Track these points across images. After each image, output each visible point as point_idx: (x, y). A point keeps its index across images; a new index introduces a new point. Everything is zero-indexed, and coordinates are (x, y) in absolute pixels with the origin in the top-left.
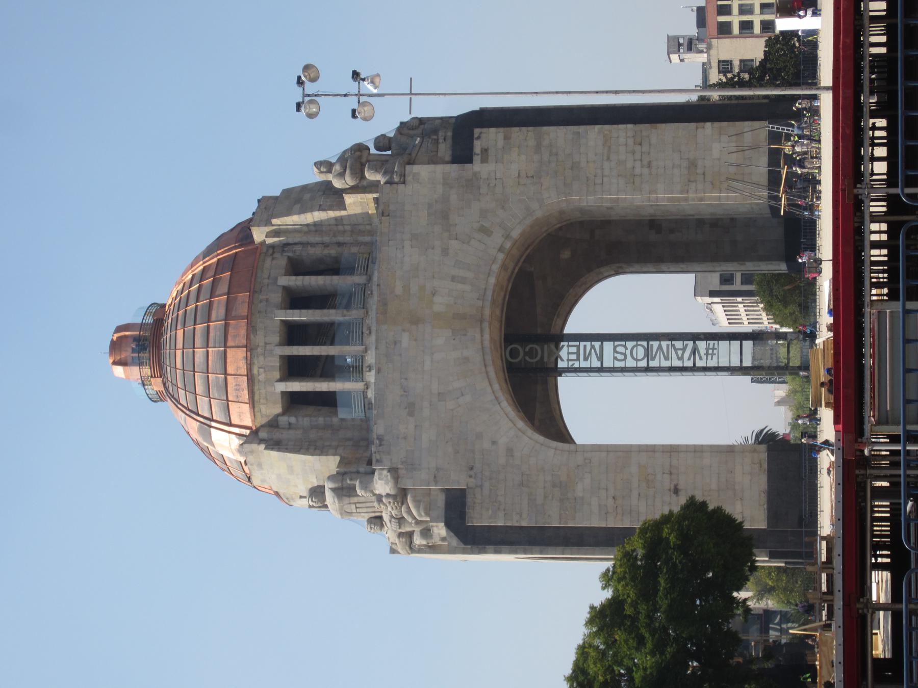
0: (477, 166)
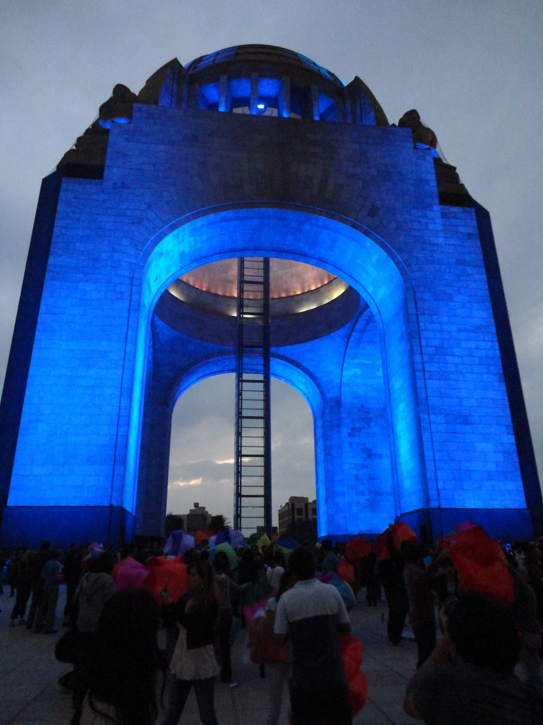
0: (437, 208)
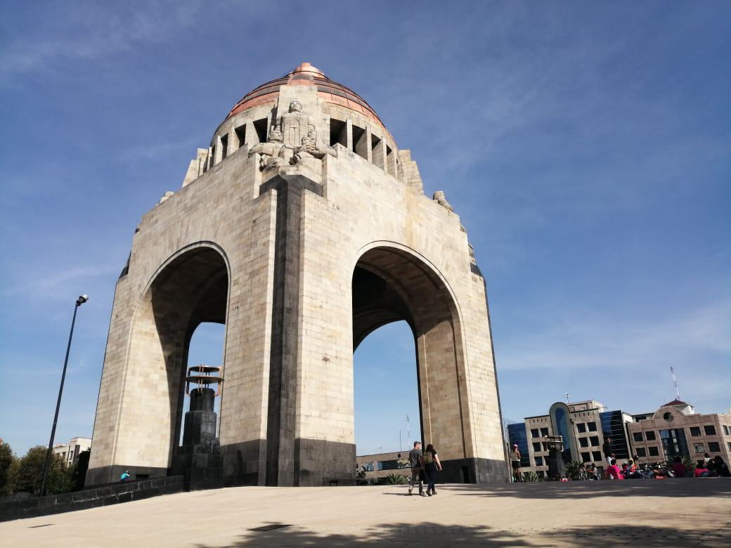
0: (471, 274)
